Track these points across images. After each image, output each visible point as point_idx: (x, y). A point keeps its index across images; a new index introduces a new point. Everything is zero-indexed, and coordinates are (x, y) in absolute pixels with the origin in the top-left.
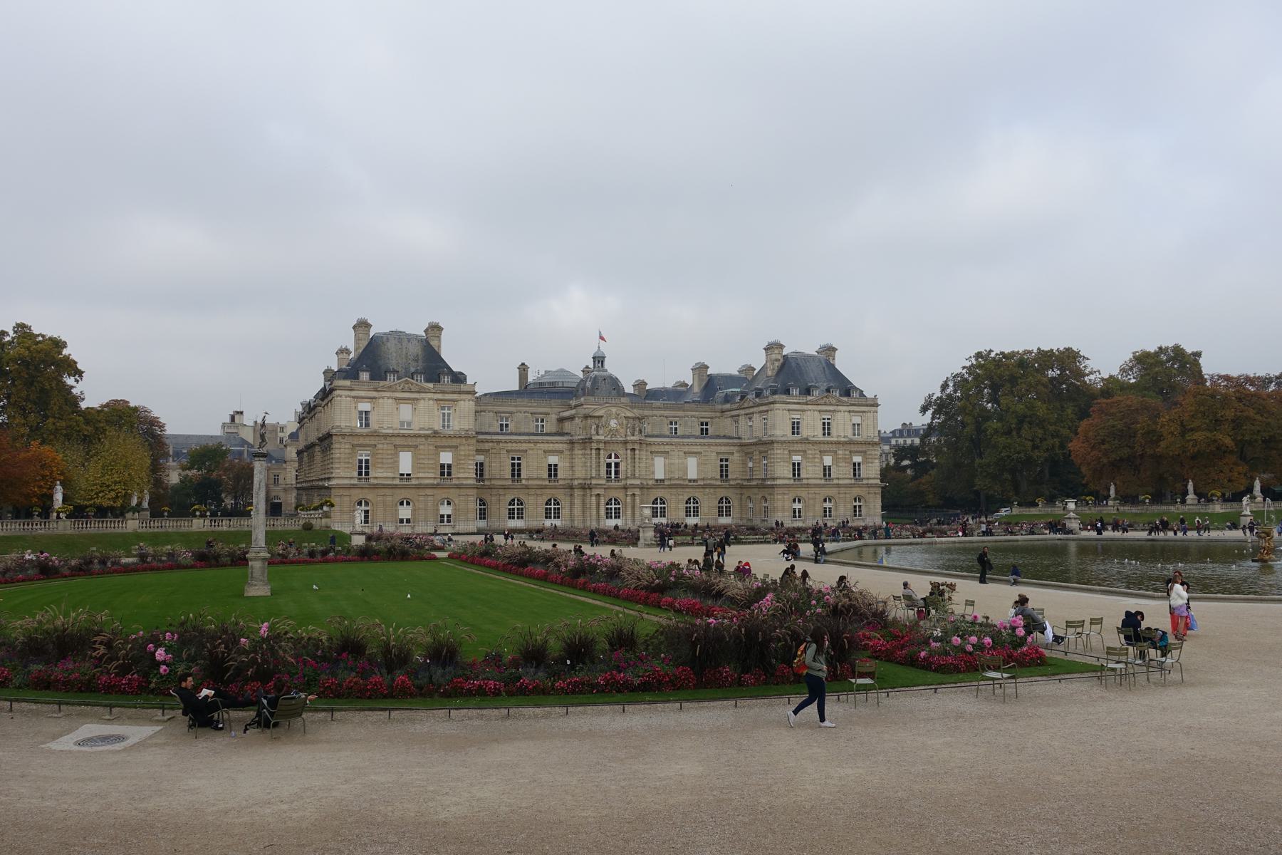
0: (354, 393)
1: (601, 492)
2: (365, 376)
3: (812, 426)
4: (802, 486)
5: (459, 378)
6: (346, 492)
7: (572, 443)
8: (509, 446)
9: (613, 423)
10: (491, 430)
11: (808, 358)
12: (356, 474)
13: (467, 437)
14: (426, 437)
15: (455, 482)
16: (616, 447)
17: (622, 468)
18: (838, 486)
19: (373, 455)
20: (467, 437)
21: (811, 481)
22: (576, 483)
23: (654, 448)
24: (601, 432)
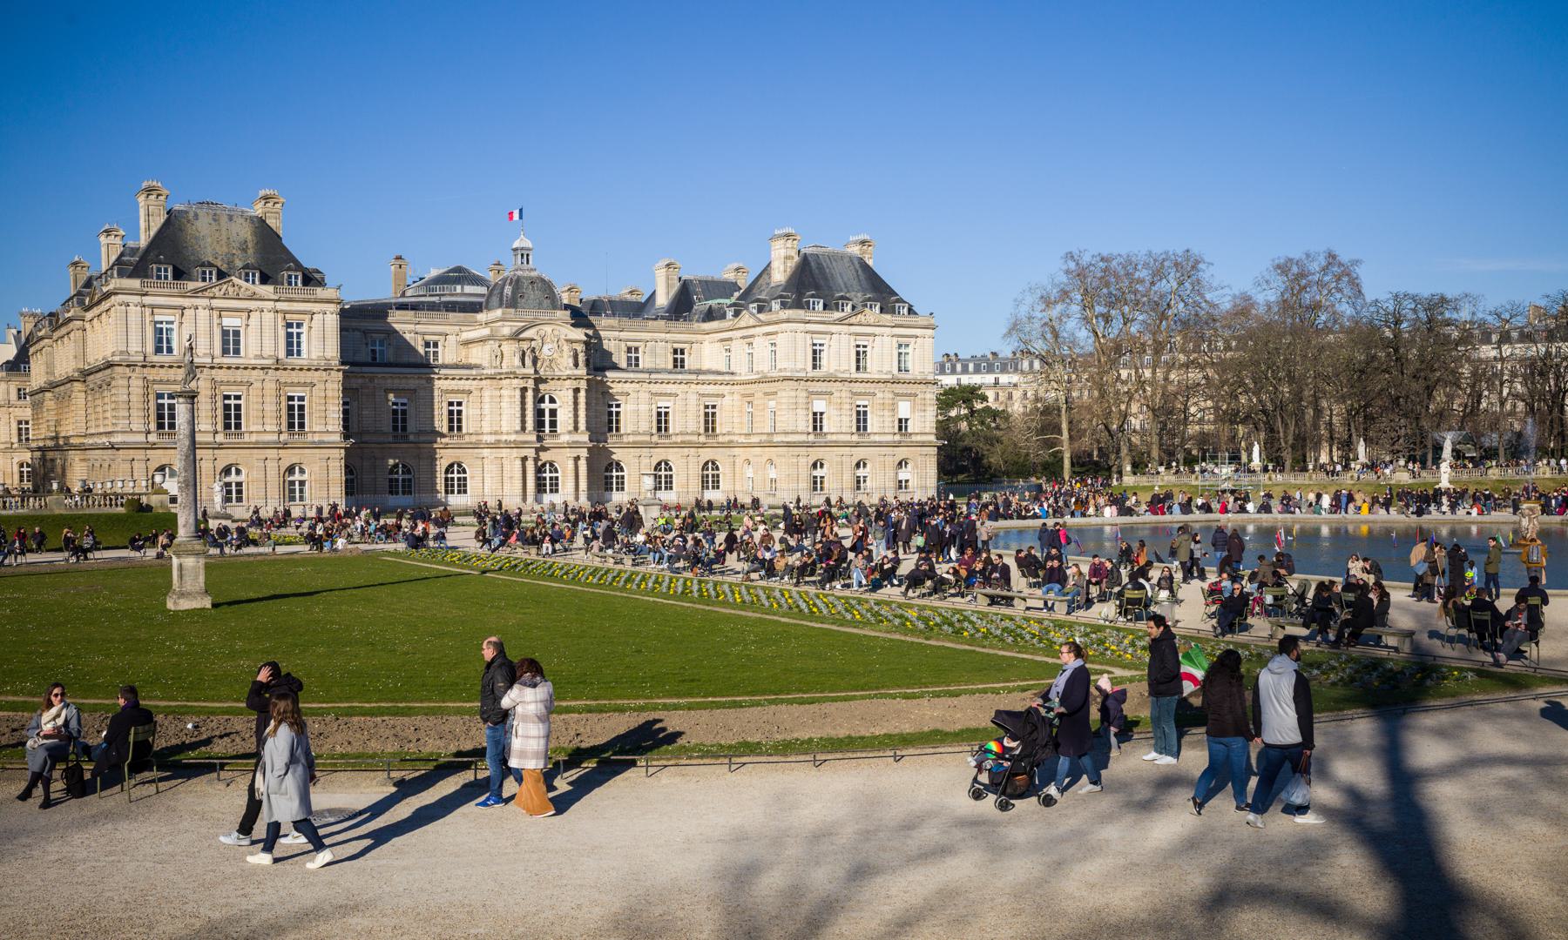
0: (147, 300)
3: (838, 357)
5: (311, 279)
6: (140, 455)
17: (560, 418)
22: (491, 439)
24: (528, 361)
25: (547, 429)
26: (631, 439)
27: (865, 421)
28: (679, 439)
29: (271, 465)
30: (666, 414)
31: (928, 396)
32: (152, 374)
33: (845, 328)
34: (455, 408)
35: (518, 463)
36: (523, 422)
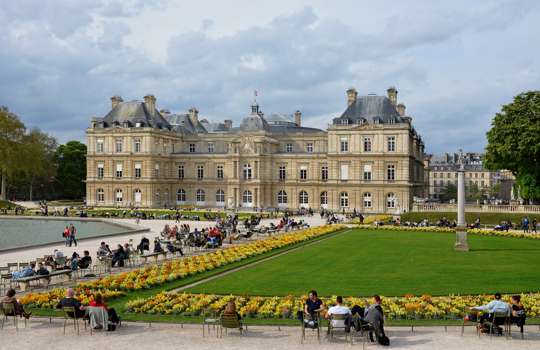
0: (95, 135)
1: (238, 187)
2: (101, 126)
3: (356, 144)
4: (345, 186)
6: (92, 185)
7: (228, 158)
8: (196, 160)
9: (247, 146)
10: (203, 151)
11: (370, 98)
12: (97, 176)
13: (146, 156)
14: (127, 156)
15: (141, 180)
16: (248, 160)
18: (374, 186)
19: (104, 166)
20: (146, 156)
21: (352, 182)
22: (229, 181)
23: (278, 161)
25: (247, 177)
26: (288, 182)
27: (369, 174)
28: (309, 182)
29: (129, 189)
30: (305, 171)
31: (404, 162)
32: (96, 159)
33: (358, 132)
34: (220, 169)
35: (233, 190)
36: (235, 174)
